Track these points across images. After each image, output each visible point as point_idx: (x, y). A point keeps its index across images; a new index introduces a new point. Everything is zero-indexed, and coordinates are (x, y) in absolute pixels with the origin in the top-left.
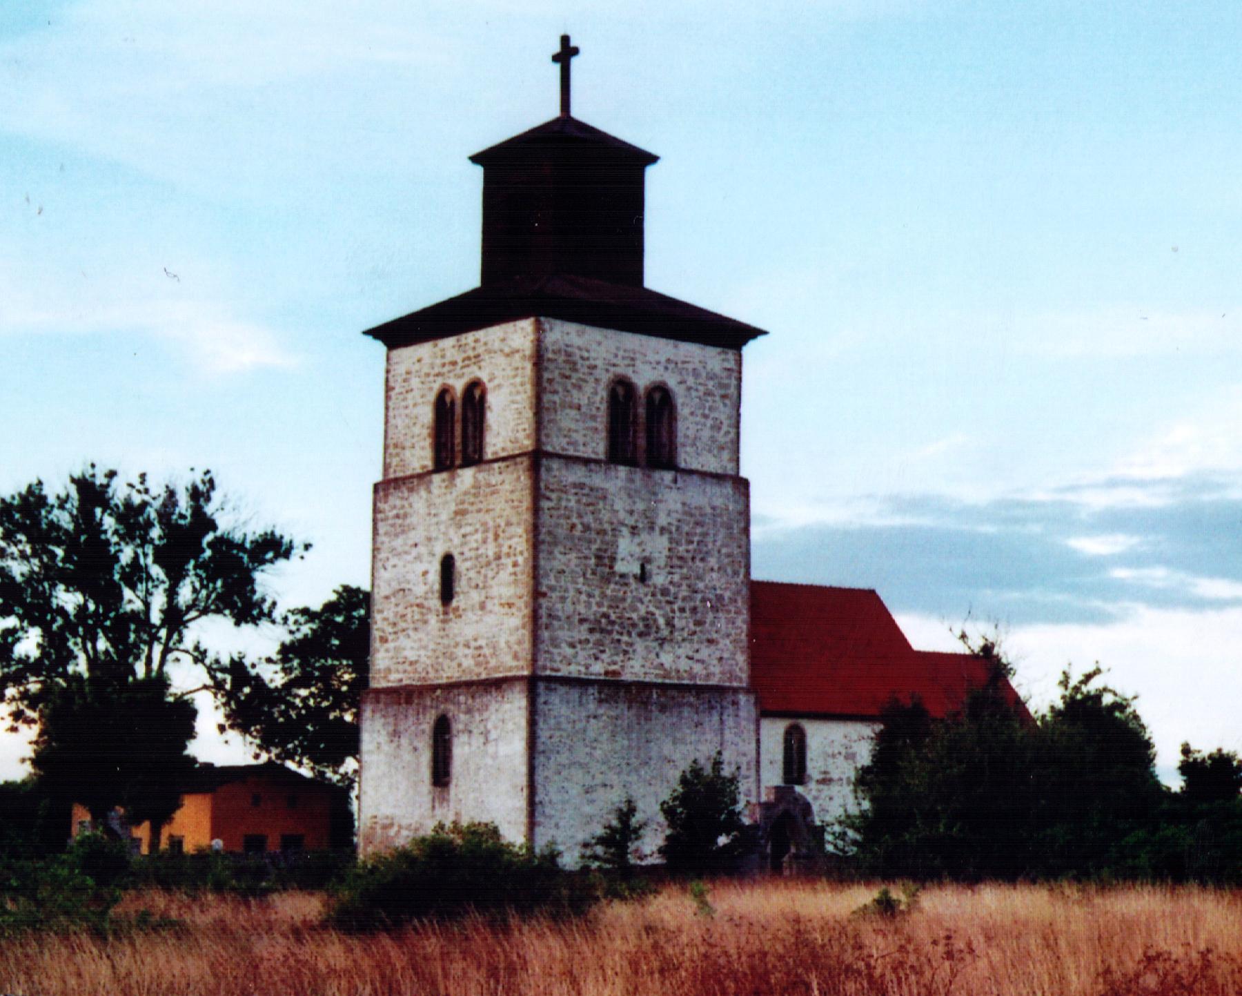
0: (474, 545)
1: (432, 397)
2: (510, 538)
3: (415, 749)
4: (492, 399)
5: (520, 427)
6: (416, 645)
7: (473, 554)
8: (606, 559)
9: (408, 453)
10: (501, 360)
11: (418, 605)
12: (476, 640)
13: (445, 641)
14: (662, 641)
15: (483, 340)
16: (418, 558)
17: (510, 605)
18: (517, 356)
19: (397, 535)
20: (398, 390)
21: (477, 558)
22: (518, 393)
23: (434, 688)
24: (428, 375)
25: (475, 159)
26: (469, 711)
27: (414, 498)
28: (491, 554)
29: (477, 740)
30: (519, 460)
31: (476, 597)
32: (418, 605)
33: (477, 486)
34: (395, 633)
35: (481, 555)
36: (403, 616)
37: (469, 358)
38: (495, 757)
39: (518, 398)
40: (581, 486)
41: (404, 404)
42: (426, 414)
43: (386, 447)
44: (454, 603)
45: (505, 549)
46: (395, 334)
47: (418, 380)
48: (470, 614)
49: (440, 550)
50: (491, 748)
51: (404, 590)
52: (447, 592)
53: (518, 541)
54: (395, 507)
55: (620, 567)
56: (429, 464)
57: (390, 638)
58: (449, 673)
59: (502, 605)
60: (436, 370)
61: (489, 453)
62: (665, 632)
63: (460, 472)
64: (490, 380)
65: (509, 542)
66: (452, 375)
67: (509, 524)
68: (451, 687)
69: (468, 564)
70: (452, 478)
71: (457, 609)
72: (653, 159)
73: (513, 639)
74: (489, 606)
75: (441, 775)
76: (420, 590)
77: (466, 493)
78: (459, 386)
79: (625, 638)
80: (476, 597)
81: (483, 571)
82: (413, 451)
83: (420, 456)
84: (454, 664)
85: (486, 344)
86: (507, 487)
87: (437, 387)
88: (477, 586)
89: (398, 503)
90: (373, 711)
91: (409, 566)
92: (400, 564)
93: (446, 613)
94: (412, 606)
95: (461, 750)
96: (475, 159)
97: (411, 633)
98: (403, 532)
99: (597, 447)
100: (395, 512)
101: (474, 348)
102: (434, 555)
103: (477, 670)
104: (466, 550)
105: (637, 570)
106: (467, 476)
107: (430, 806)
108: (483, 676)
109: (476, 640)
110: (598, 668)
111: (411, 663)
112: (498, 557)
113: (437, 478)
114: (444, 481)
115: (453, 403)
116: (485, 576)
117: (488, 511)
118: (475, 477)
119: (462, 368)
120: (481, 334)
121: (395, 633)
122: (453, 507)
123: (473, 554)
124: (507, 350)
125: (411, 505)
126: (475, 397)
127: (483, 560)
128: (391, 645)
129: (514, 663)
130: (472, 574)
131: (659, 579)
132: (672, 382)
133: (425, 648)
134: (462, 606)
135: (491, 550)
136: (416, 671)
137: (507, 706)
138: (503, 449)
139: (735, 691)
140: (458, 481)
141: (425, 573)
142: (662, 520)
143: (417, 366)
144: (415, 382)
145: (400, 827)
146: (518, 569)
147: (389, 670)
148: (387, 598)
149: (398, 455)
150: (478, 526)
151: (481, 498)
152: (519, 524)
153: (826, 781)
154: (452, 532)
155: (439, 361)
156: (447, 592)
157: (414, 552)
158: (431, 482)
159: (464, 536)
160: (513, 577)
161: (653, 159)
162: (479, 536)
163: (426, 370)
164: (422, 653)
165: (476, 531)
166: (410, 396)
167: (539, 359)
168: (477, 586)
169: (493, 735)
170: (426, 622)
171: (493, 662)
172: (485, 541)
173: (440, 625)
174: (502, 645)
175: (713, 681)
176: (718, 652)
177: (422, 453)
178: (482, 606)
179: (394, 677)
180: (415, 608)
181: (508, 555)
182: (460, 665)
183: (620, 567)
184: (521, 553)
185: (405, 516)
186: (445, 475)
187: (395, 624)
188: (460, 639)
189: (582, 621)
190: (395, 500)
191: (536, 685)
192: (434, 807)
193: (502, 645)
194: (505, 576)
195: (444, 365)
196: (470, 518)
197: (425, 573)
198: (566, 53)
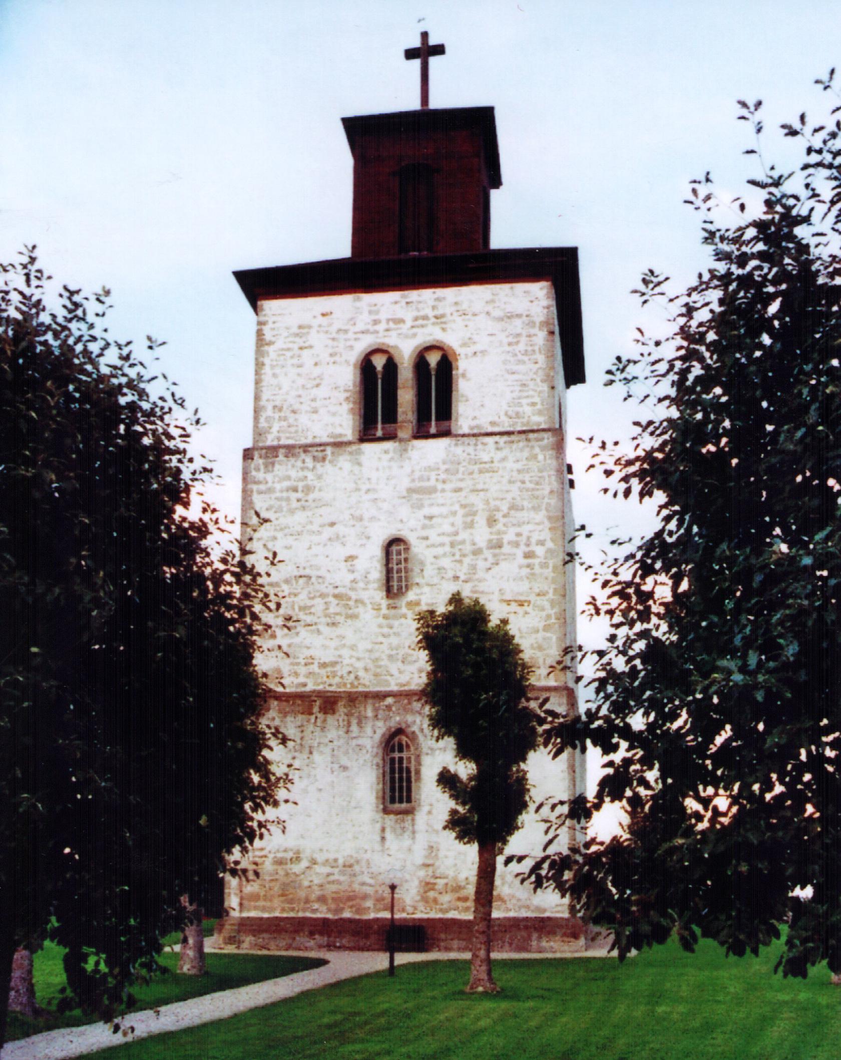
3: (345, 768)
4: (463, 365)
6: (333, 644)
11: (336, 596)
18: (518, 322)
19: (292, 512)
20: (280, 344)
27: (327, 469)
28: (482, 543)
30: (531, 436)
32: (336, 596)
35: (463, 542)
37: (425, 318)
39: (521, 368)
45: (510, 536)
51: (309, 577)
54: (288, 478)
59: (508, 602)
64: (464, 345)
67: (513, 507)
69: (440, 551)
77: (430, 469)
82: (315, 416)
85: (456, 303)
86: (510, 464)
89: (293, 473)
93: (390, 607)
100: (286, 484)
101: (434, 308)
102: (368, 538)
104: (433, 534)
107: (378, 838)
111: (323, 665)
116: (474, 567)
119: (413, 327)
122: (406, 483)
123: (447, 540)
124: (497, 313)
125: (319, 477)
127: (468, 548)
130: (446, 562)
135: (482, 535)
138: (493, 423)
143: (324, 321)
144: (315, 338)
145: (314, 862)
146: (536, 561)
150: (457, 507)
151: (460, 476)
154: (404, 511)
157: (328, 532)
158: (359, 452)
159: (431, 518)
160: (525, 571)
162: (459, 520)
163: (337, 325)
165: (454, 513)
166: (305, 352)
173: (381, 620)
180: (331, 599)
181: (517, 545)
184: (541, 543)
185: (308, 489)
192: (383, 838)
195: (376, 322)
196: (438, 497)
197: (350, 558)
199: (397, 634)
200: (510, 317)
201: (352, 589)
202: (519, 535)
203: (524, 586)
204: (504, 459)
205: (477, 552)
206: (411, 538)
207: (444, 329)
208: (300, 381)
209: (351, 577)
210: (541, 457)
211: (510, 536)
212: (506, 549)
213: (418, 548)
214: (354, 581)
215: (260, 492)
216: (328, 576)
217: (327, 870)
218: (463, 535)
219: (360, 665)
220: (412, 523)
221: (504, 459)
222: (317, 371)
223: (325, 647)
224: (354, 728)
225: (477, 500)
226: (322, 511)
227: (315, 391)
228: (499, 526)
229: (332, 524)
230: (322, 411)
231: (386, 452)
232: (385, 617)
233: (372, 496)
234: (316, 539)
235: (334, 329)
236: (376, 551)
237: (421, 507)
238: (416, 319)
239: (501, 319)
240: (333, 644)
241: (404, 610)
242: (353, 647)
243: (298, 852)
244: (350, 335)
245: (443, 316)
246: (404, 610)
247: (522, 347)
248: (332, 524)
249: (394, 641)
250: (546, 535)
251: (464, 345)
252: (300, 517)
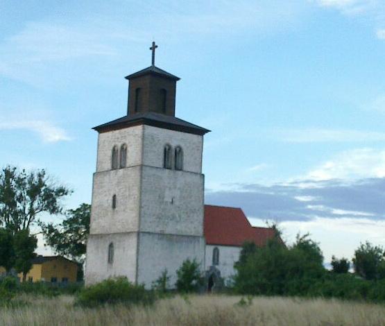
1: (111, 148)
4: (129, 149)
8: (161, 197)
14: (177, 222)
23: (109, 235)
25: (127, 78)
26: (120, 241)
29: (121, 250)
31: (122, 207)
33: (124, 174)
40: (154, 175)
42: (110, 153)
43: (97, 163)
44: (116, 209)
46: (101, 129)
52: (114, 206)
53: (136, 191)
55: (166, 199)
58: (114, 230)
61: (128, 165)
62: (179, 219)
67: (133, 186)
72: (178, 79)
75: (110, 260)
76: (106, 205)
78: (119, 145)
79: (167, 221)
80: (122, 207)
83: (108, 165)
87: (113, 145)
95: (116, 252)
96: (127, 78)
99: (160, 163)
105: (171, 201)
110: (158, 230)
112: (129, 195)
113: (112, 172)
120: (126, 130)
126: (124, 149)
128: (97, 221)
131: (177, 203)
132: (182, 145)
135: (127, 193)
139: (199, 237)
140: (118, 173)
141: (108, 200)
142: (178, 186)
153: (225, 264)
156: (114, 206)
161: (178, 79)
167: (143, 138)
170: (107, 215)
172: (125, 191)
175: (192, 234)
176: (195, 225)
178: (124, 210)
179: (97, 231)
183: (166, 199)
186: (114, 171)
189: (154, 215)
190: (99, 178)
191: (139, 233)
193: (130, 222)
197: (108, 200)
198: (154, 47)
237: (118, 186)
250: (137, 193)
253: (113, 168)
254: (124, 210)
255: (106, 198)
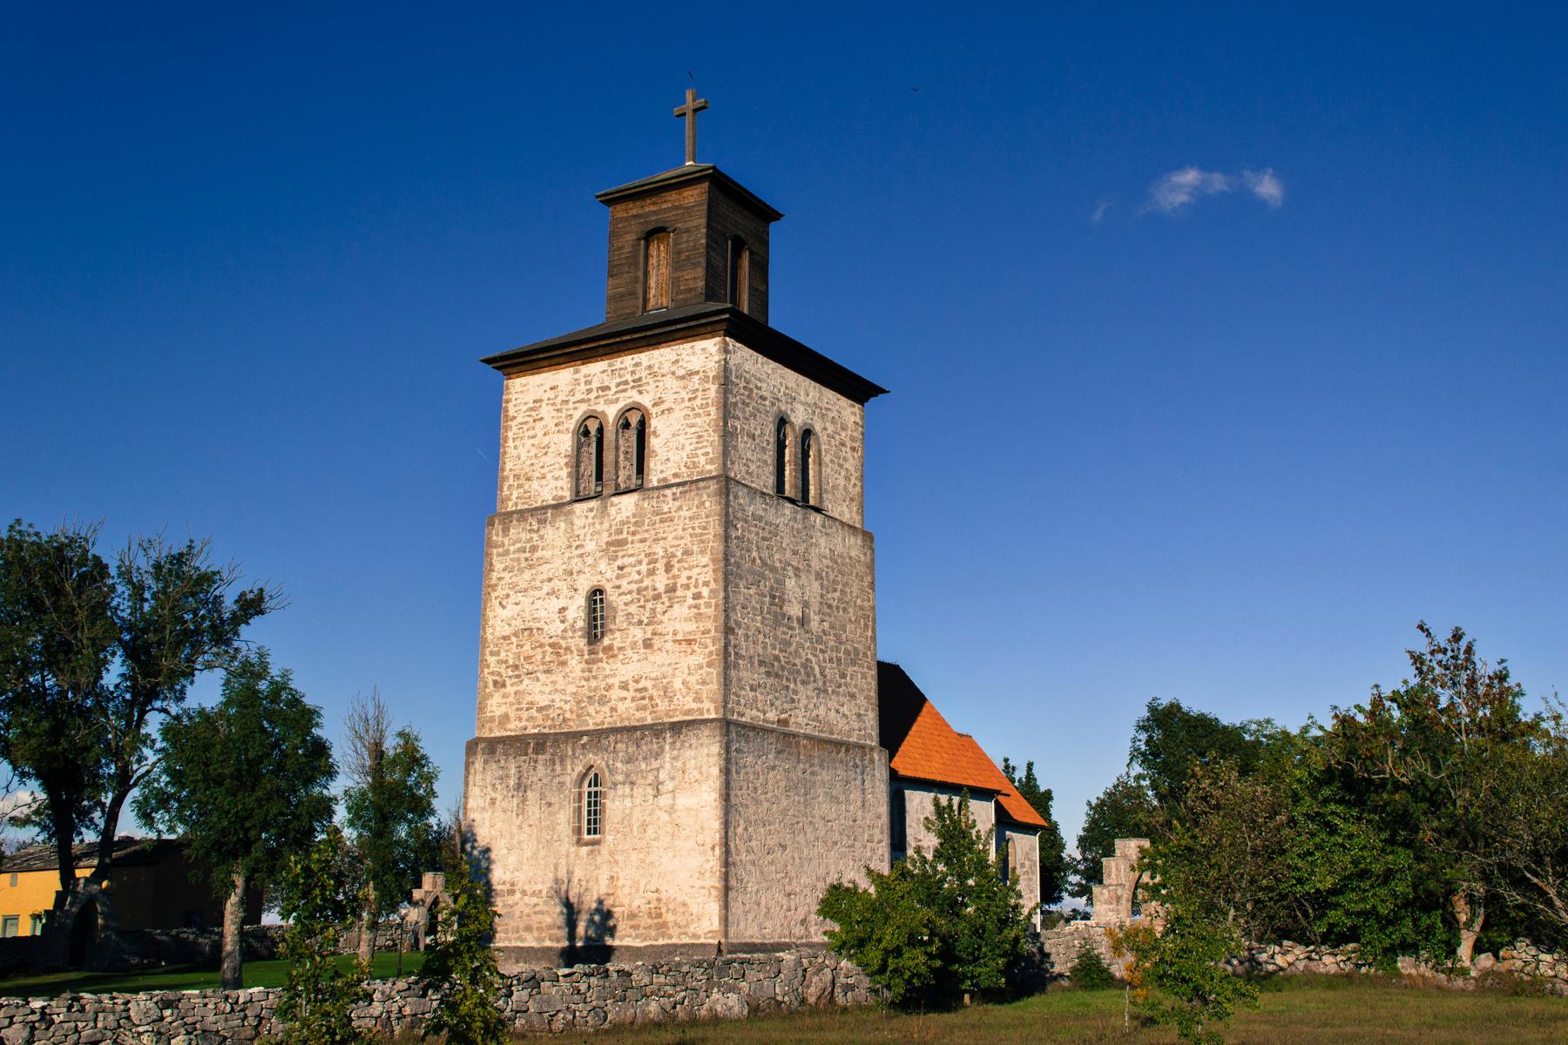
0: (637, 577)
1: (571, 425)
2: (690, 568)
4: (654, 423)
5: (699, 452)
6: (547, 690)
7: (634, 587)
9: (535, 485)
10: (670, 382)
11: (551, 645)
12: (637, 682)
13: (593, 683)
15: (645, 363)
16: (552, 593)
17: (689, 642)
18: (696, 378)
19: (521, 571)
20: (520, 419)
21: (639, 591)
22: (698, 415)
23: (578, 735)
24: (567, 402)
26: (629, 760)
27: (549, 532)
28: (661, 588)
29: (643, 791)
30: (701, 484)
31: (638, 634)
32: (551, 645)
34: (518, 676)
35: (646, 588)
36: (527, 658)
37: (626, 383)
38: (671, 810)
39: (698, 420)
41: (531, 433)
42: (566, 443)
44: (606, 641)
45: (683, 580)
47: (551, 408)
48: (629, 652)
49: (585, 584)
50: (665, 800)
53: (702, 571)
54: (518, 541)
56: (567, 495)
57: (508, 682)
58: (597, 717)
59: (679, 642)
60: (579, 396)
61: (653, 479)
63: (615, 500)
64: (655, 405)
65: (685, 574)
66: (601, 400)
67: (687, 553)
68: (599, 736)
69: (629, 597)
70: (604, 511)
71: (610, 648)
72: (777, 216)
73: (692, 679)
74: (657, 642)
77: (623, 523)
78: (611, 413)
80: (638, 634)
81: (649, 605)
82: (544, 482)
84: (606, 709)
85: (650, 367)
86: (684, 513)
87: (578, 415)
88: (640, 622)
89: (524, 536)
90: (486, 762)
91: (539, 604)
92: (526, 601)
93: (591, 652)
94: (542, 646)
97: (542, 677)
98: (531, 567)
100: (518, 545)
101: (633, 372)
103: (639, 715)
104: (624, 583)
106: (628, 503)
108: (649, 721)
109: (637, 682)
111: (540, 710)
112: (671, 589)
113: (578, 507)
114: (591, 510)
115: (601, 430)
116: (653, 610)
117: (656, 540)
118: (637, 505)
121: (518, 676)
122: (605, 537)
123: (634, 587)
124: (681, 372)
125: (542, 537)
126: (638, 427)
127: (650, 593)
128: (510, 689)
129: (694, 706)
130: (633, 609)
133: (563, 691)
134: (616, 644)
135: (661, 581)
136: (547, 717)
137: (689, 753)
138: (675, 475)
143: (551, 394)
144: (546, 411)
145: (524, 893)
146: (701, 601)
147: (505, 718)
148: (505, 638)
149: (520, 486)
152: (702, 552)
154: (603, 566)
155: (583, 387)
158: (572, 512)
159: (621, 568)
161: (777, 216)
162: (644, 568)
163: (562, 397)
164: (557, 697)
165: (640, 562)
166: (539, 425)
167: (726, 379)
168: (640, 622)
169: (669, 786)
171: (662, 706)
172: (651, 573)
173: (583, 665)
174: (677, 684)
177: (559, 483)
181: (687, 587)
182: (613, 709)
184: (706, 584)
185: (534, 549)
186: (593, 504)
187: (516, 667)
188: (615, 681)
191: (730, 729)
193: (677, 684)
194: (681, 611)
195: (589, 391)
196: (630, 549)
197: (563, 609)
199: (595, 677)
200: (692, 373)
201: (564, 638)
202: (689, 578)
203: (692, 626)
204: (680, 508)
205: (657, 597)
206: (608, 587)
207: (640, 392)
208: (534, 451)
209: (562, 626)
210: (707, 504)
211: (683, 580)
212: (679, 593)
213: (612, 596)
214: (565, 631)
215: (499, 555)
216: (546, 628)
217: (535, 900)
218: (647, 582)
219: (567, 707)
220: (609, 575)
221: (680, 508)
222: (546, 440)
223: (542, 692)
224: (558, 768)
225: (659, 550)
226: (545, 568)
227: (544, 459)
228: (675, 571)
229: (550, 580)
230: (549, 476)
231: (591, 510)
232: (587, 662)
233: (580, 551)
234: (537, 594)
235: (558, 401)
236: (581, 600)
237: (615, 558)
238: (618, 385)
239: (683, 378)
240: (547, 690)
241: (601, 655)
242: (563, 691)
243: (513, 884)
244: (571, 405)
245: (640, 379)
246: (601, 655)
247: (698, 402)
248: (550, 580)
249: (593, 683)
250: (710, 576)
251: (655, 405)
252: (527, 575)
253: (579, 498)
254: (648, 644)
255: (555, 604)
